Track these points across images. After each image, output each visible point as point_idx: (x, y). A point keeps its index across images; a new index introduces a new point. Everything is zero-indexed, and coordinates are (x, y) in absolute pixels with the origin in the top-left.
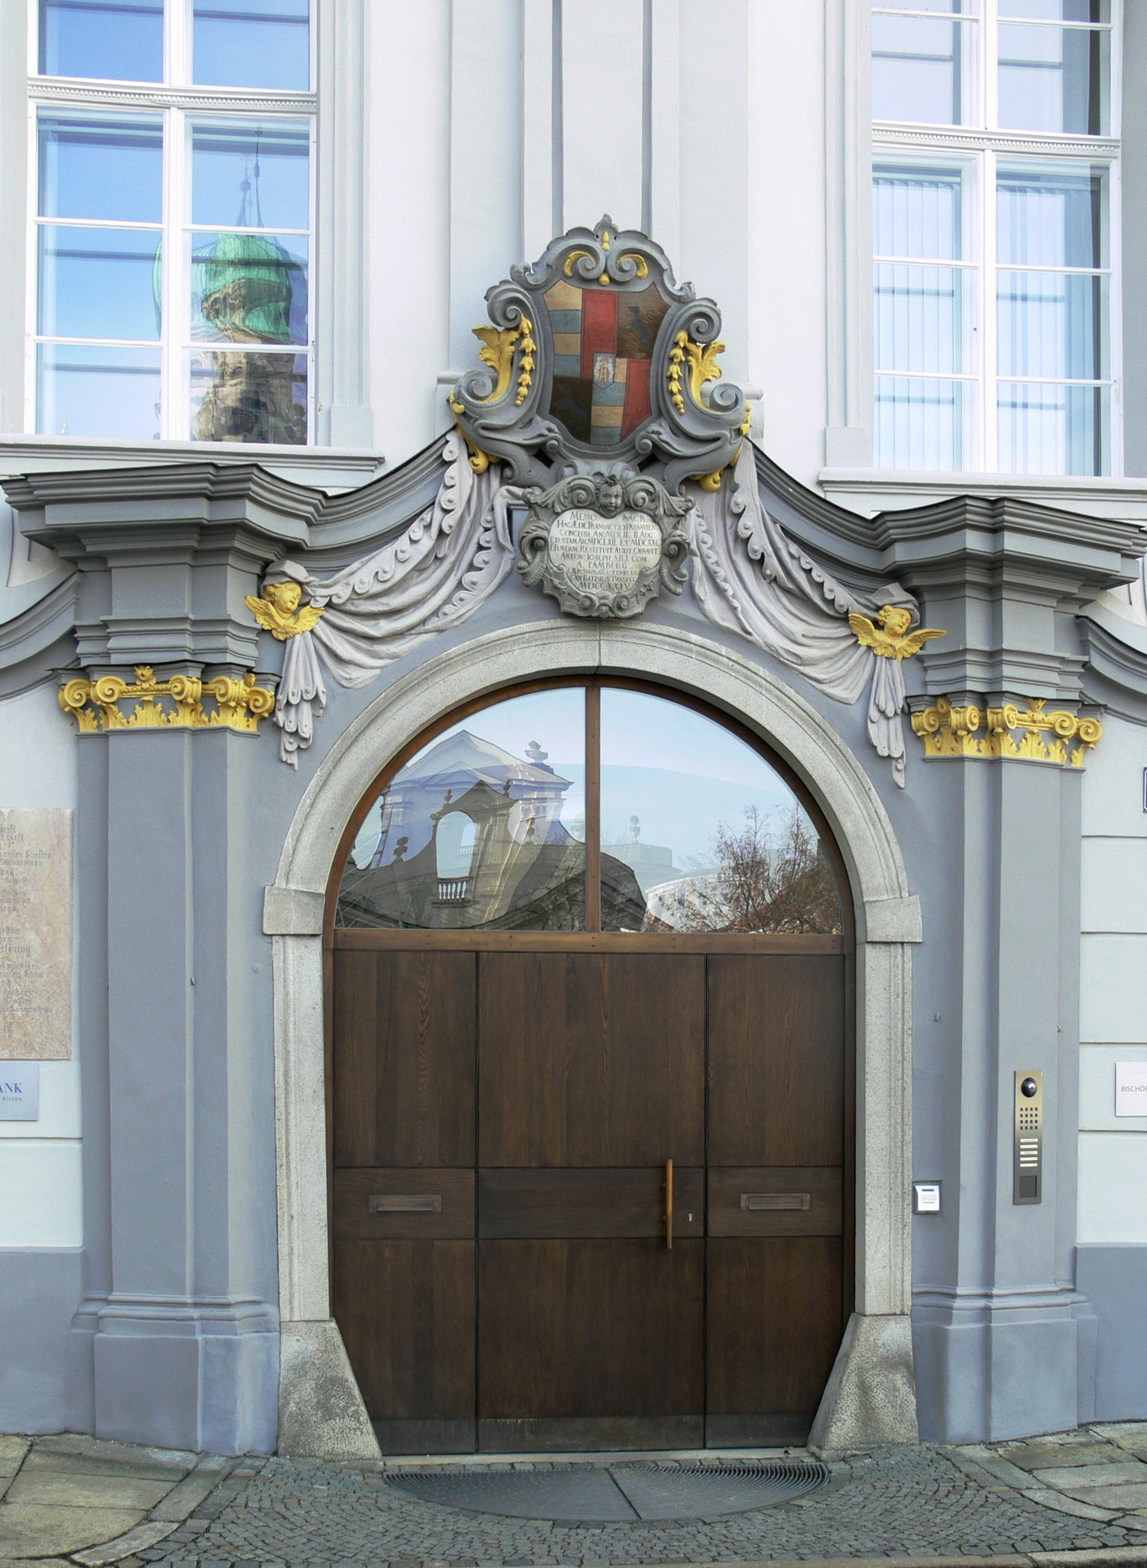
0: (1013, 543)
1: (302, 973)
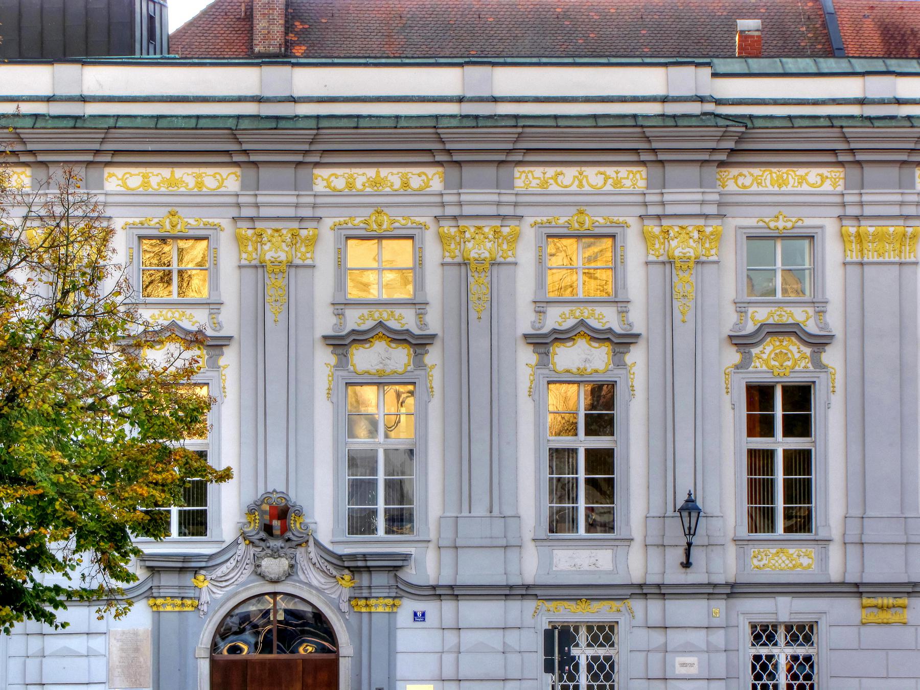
0: (369, 564)
1: (204, 667)
